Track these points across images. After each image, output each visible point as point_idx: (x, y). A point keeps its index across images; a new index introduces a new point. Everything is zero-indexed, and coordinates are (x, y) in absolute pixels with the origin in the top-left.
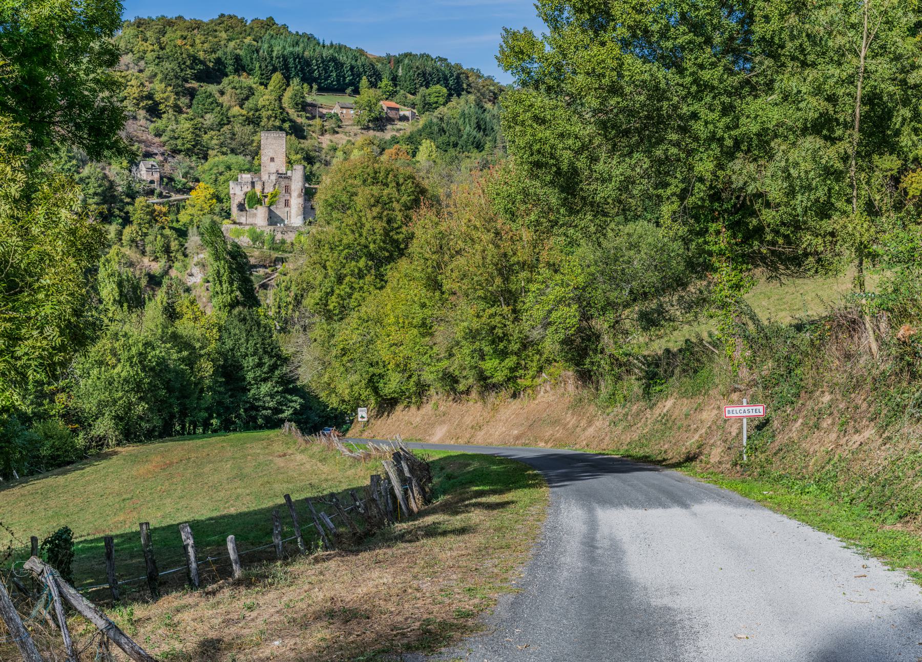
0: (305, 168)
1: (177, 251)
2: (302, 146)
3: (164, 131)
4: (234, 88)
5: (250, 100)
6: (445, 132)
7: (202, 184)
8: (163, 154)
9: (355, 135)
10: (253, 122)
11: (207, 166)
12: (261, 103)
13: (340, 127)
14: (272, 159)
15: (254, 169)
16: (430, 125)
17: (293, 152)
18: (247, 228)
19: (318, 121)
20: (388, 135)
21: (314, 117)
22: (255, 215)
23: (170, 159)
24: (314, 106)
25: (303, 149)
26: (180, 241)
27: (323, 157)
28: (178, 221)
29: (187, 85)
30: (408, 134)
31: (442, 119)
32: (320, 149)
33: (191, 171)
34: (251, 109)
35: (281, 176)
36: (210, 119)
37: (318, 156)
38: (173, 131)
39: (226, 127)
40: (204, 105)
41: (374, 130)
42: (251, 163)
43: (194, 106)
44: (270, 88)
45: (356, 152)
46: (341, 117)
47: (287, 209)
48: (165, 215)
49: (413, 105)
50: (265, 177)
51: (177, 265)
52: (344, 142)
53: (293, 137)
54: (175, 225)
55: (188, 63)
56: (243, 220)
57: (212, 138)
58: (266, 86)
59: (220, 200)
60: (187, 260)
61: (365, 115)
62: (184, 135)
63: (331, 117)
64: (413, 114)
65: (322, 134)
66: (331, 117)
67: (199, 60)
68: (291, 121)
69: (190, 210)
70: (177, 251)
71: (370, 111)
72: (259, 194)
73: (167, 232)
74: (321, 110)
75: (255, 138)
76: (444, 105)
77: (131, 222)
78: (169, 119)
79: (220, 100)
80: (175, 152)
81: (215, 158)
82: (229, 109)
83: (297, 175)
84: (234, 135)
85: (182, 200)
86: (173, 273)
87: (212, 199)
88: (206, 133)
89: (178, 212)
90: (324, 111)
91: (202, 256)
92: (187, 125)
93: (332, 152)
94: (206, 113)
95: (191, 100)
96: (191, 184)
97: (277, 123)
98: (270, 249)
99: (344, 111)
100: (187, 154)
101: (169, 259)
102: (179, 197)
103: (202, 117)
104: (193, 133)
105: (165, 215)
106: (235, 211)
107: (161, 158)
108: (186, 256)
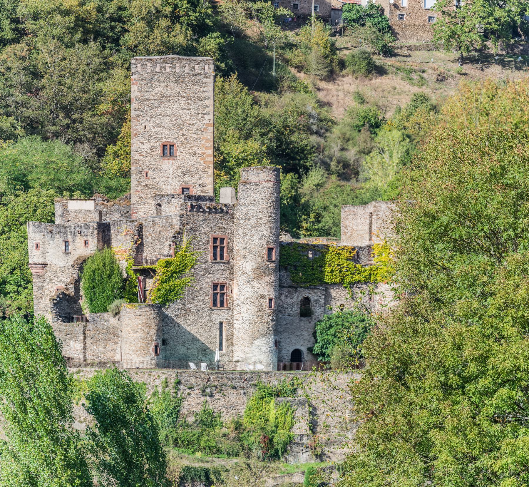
2: (265, 112)
9: (441, 79)
10: (98, 34)
13: (388, 52)
25: (265, 123)
27: (335, 149)
37: (319, 149)
41: (502, 63)
46: (394, 22)
47: (219, 315)
52: (405, 102)
63: (360, 21)
66: (360, 21)
75: (107, 86)
84: (36, 75)
93: (364, 135)
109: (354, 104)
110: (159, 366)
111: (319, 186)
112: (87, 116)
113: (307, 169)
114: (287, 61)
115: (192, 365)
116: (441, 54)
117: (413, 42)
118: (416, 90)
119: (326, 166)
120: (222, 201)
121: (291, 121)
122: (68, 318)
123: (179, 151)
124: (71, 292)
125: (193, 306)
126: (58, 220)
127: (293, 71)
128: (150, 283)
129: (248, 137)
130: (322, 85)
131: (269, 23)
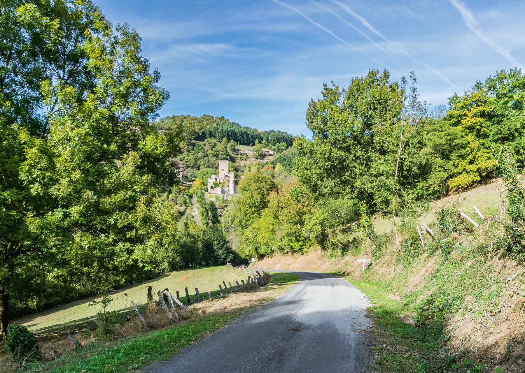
1: (189, 203)
3: (183, 159)
4: (209, 143)
5: (215, 148)
6: (286, 160)
8: (183, 168)
11: (199, 172)
12: (219, 149)
13: (247, 158)
15: (216, 173)
16: (280, 157)
17: (230, 167)
18: (214, 195)
19: (239, 156)
20: (265, 161)
21: (238, 154)
23: (186, 169)
24: (238, 150)
27: (241, 169)
28: (189, 192)
29: (192, 142)
30: (272, 161)
31: (284, 155)
32: (241, 166)
35: (226, 176)
36: (200, 155)
38: (187, 159)
42: (215, 171)
44: (222, 143)
45: (253, 167)
47: (228, 188)
48: (184, 190)
49: (274, 150)
50: (220, 176)
51: (189, 208)
52: (249, 164)
53: (231, 161)
54: (188, 194)
55: (192, 133)
56: (212, 192)
58: (221, 142)
59: (204, 185)
61: (257, 154)
62: (191, 161)
64: (274, 153)
65: (241, 161)
67: (196, 132)
68: (230, 155)
69: (193, 188)
70: (189, 203)
71: (258, 152)
72: (218, 183)
73: (185, 196)
76: (285, 150)
77: (172, 193)
79: (204, 148)
80: (188, 167)
81: (203, 169)
82: (207, 151)
83: (232, 175)
86: (188, 211)
89: (189, 189)
90: (242, 152)
92: (192, 157)
95: (193, 147)
97: (225, 156)
99: (249, 152)
100: (192, 168)
101: (186, 206)
102: (189, 183)
105: (184, 190)
106: (209, 189)
107: (183, 169)
108: (192, 205)
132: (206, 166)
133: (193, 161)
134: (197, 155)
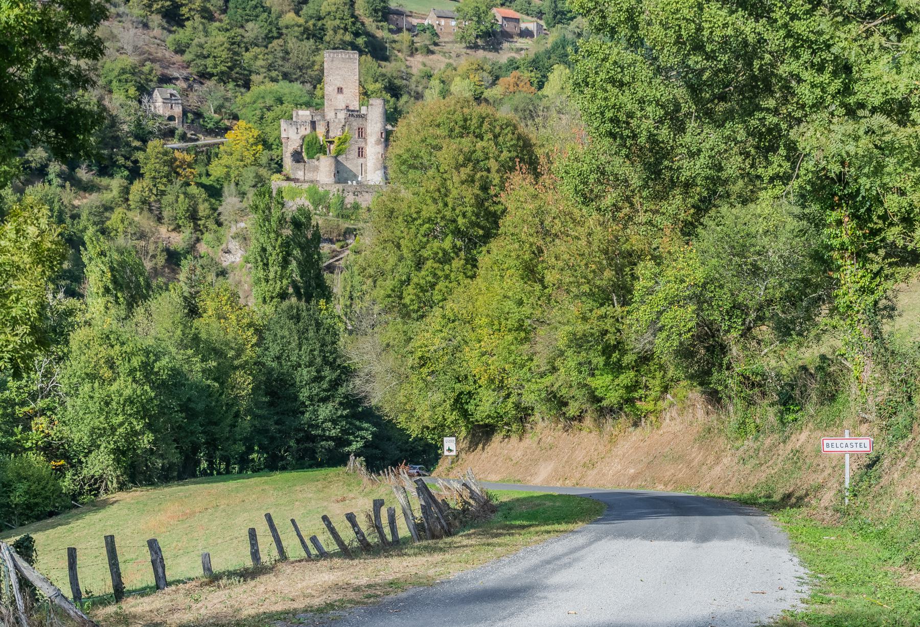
0: (386, 101)
1: (208, 217)
2: (384, 70)
7: (242, 123)
9: (458, 56)
10: (314, 36)
13: (436, 44)
14: (340, 90)
17: (370, 79)
18: (305, 186)
22: (316, 169)
23: (196, 86)
25: (384, 75)
26: (211, 204)
27: (413, 86)
28: (208, 175)
33: (227, 104)
34: (311, 17)
37: (407, 86)
38: (201, 46)
39: (275, 42)
40: (244, 9)
41: (484, 49)
43: (231, 11)
45: (458, 79)
46: (438, 31)
47: (361, 160)
52: (443, 66)
54: (204, 180)
57: (256, 58)
60: (222, 230)
62: (217, 52)
63: (424, 30)
65: (412, 55)
66: (424, 30)
68: (368, 34)
70: (208, 217)
72: (321, 138)
74: (410, 19)
75: (317, 58)
78: (195, 28)
84: (287, 53)
85: (214, 144)
87: (256, 144)
88: (247, 50)
90: (415, 22)
91: (242, 225)
93: (425, 80)
94: (247, 21)
96: (227, 123)
98: (338, 216)
99: (443, 22)
100: (221, 80)
103: (242, 27)
104: (229, 49)
108: (220, 224)
109: (422, 67)
110: (336, 182)
111: (406, 102)
112: (309, 71)
113: (401, 95)
114: (393, 48)
115: (350, 182)
116: (457, 45)
117: (446, 40)
118: (447, 61)
119: (409, 93)
120: (362, 112)
121: (394, 75)
122: (298, 161)
123: (344, 90)
124: (299, 150)
125: (350, 157)
126: (294, 119)
127: (396, 52)
128: (332, 147)
129: (377, 81)
130: (409, 58)
131: (386, 31)
132: (274, 74)
133: (224, 55)
134: (240, 31)
